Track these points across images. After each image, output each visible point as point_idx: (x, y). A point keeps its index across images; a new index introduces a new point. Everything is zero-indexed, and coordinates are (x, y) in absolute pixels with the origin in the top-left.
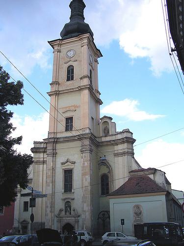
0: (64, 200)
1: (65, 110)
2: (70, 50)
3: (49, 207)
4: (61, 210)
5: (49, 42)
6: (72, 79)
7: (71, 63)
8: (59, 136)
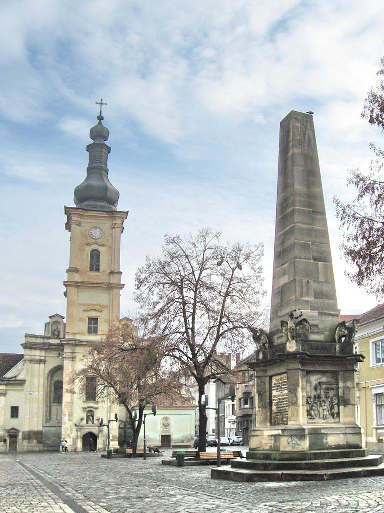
2: (96, 228)
6: (98, 270)
7: (95, 247)
8: (79, 337)
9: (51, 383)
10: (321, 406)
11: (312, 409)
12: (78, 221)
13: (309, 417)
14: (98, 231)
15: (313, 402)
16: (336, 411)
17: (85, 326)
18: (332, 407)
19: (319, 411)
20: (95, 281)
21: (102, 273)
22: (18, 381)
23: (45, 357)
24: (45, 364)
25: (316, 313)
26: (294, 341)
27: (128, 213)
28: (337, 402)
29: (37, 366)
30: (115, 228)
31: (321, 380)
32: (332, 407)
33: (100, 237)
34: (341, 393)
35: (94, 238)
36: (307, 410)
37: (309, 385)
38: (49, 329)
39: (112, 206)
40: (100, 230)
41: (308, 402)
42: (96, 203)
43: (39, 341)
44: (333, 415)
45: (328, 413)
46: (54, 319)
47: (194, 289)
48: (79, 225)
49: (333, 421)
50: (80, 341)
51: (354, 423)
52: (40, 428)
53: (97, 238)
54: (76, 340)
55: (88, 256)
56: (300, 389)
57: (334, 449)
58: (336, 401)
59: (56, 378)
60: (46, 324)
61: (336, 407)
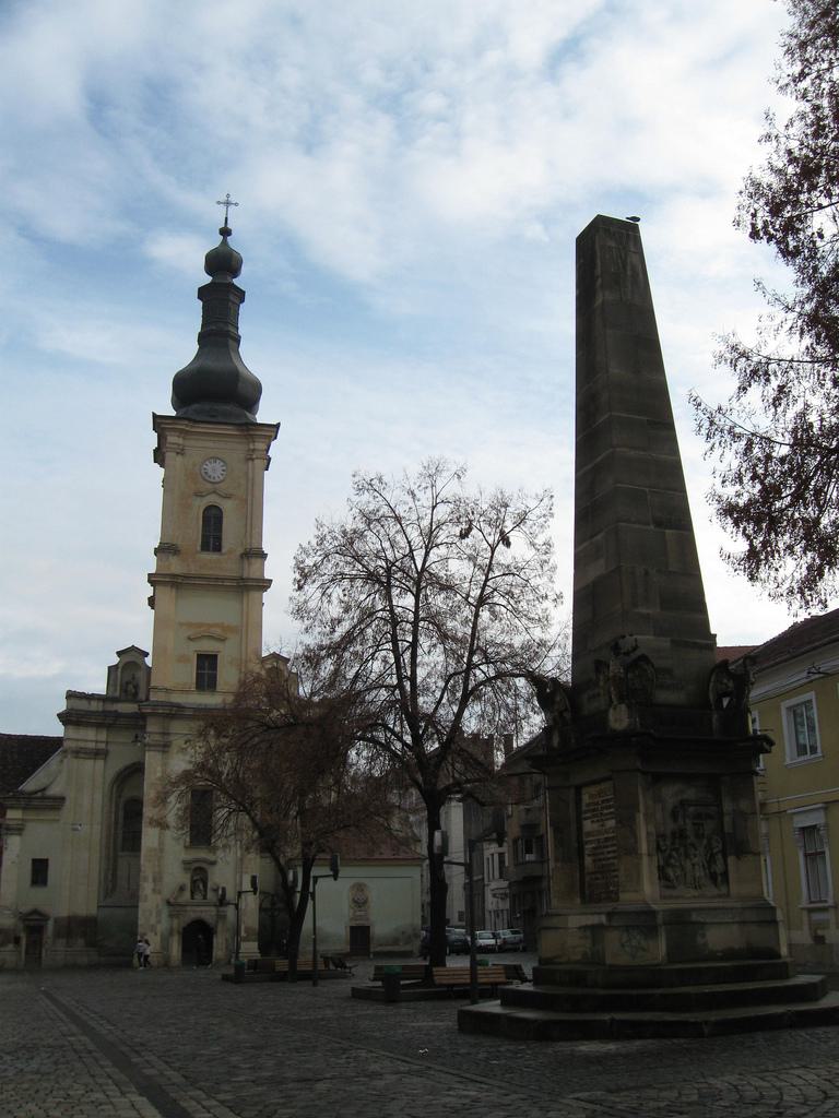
0: (186, 863)
1: (191, 632)
2: (216, 459)
3: (150, 879)
4: (182, 889)
6: (218, 549)
7: (212, 499)
8: (176, 699)
9: (117, 806)
10: (687, 856)
11: (668, 864)
12: (179, 445)
14: (218, 466)
15: (671, 848)
16: (719, 868)
17: (188, 674)
19: (683, 869)
20: (211, 572)
21: (226, 557)
22: (49, 798)
23: (107, 743)
24: (105, 759)
25: (665, 643)
26: (623, 707)
27: (278, 426)
28: (720, 846)
29: (89, 764)
30: (253, 460)
31: (685, 796)
32: (711, 860)
33: (222, 478)
34: (728, 828)
35: (212, 480)
36: (659, 866)
39: (248, 414)
41: (658, 848)
42: (216, 407)
43: (95, 706)
44: (713, 877)
45: (702, 874)
46: (128, 658)
47: (414, 590)
48: (181, 452)
49: (715, 891)
50: (179, 707)
51: (761, 896)
52: (93, 911)
53: (217, 480)
54: (172, 705)
55: (198, 519)
56: (641, 818)
57: (721, 959)
58: (717, 846)
59: (128, 793)
60: (109, 668)
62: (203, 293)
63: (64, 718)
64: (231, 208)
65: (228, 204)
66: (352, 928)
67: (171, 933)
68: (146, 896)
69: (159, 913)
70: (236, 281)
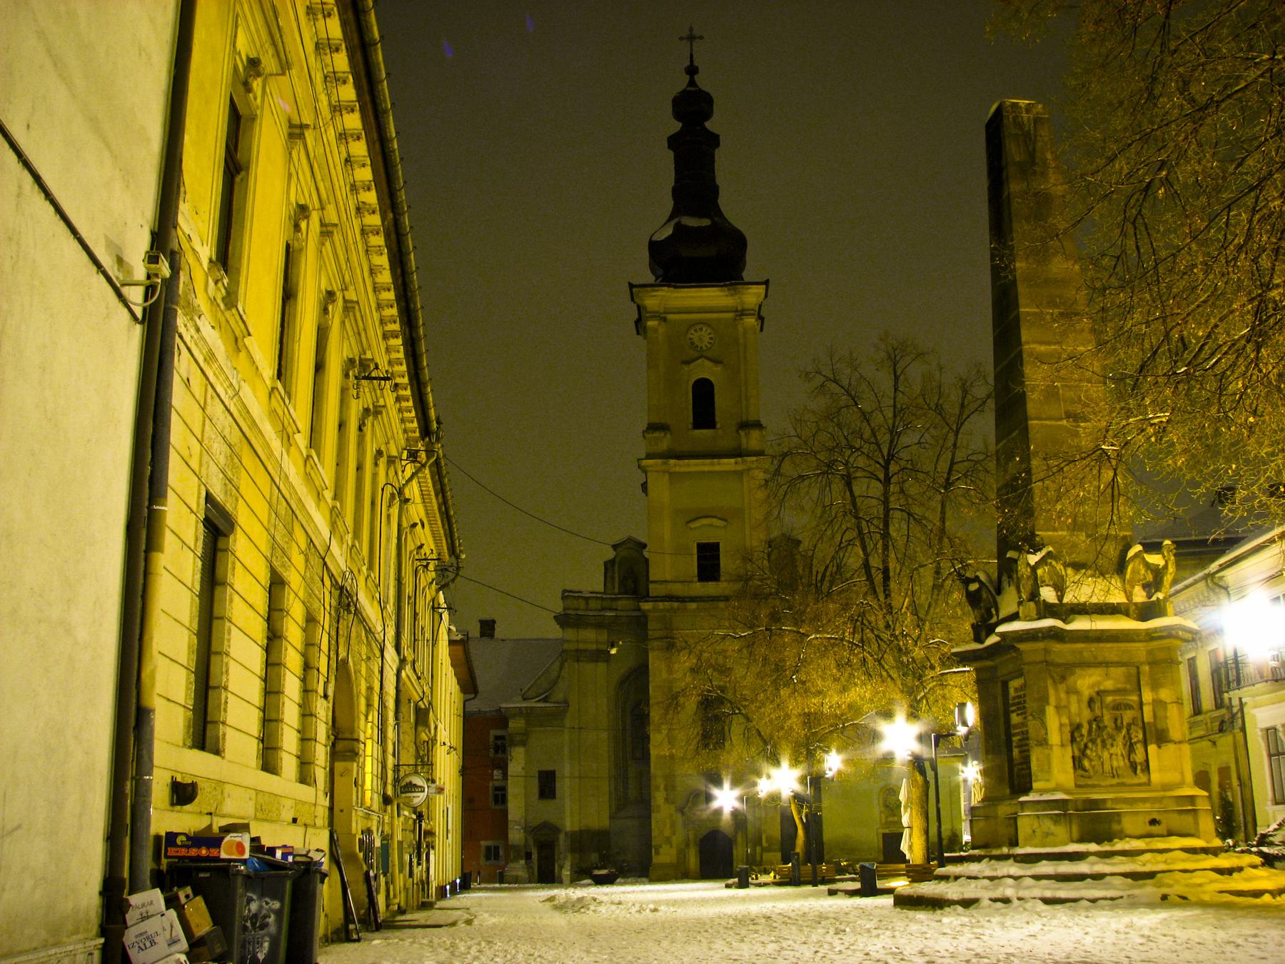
5: (631, 286)
6: (711, 424)
11: (1083, 753)
13: (1080, 772)
16: (1139, 756)
17: (691, 565)
18: (1131, 748)
29: (588, 668)
32: (1131, 748)
34: (1148, 717)
36: (1073, 757)
37: (1074, 698)
38: (613, 578)
40: (709, 331)
41: (1073, 740)
45: (1122, 763)
47: (881, 476)
56: (1050, 711)
60: (606, 564)
61: (1139, 748)
62: (673, 142)
63: (564, 620)
64: (696, 44)
65: (691, 38)
66: (884, 835)
67: (687, 845)
68: (659, 806)
69: (673, 825)
70: (708, 125)
